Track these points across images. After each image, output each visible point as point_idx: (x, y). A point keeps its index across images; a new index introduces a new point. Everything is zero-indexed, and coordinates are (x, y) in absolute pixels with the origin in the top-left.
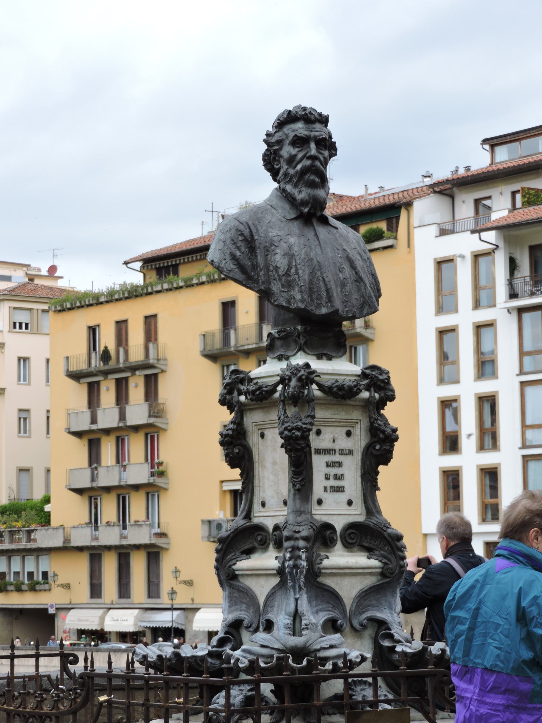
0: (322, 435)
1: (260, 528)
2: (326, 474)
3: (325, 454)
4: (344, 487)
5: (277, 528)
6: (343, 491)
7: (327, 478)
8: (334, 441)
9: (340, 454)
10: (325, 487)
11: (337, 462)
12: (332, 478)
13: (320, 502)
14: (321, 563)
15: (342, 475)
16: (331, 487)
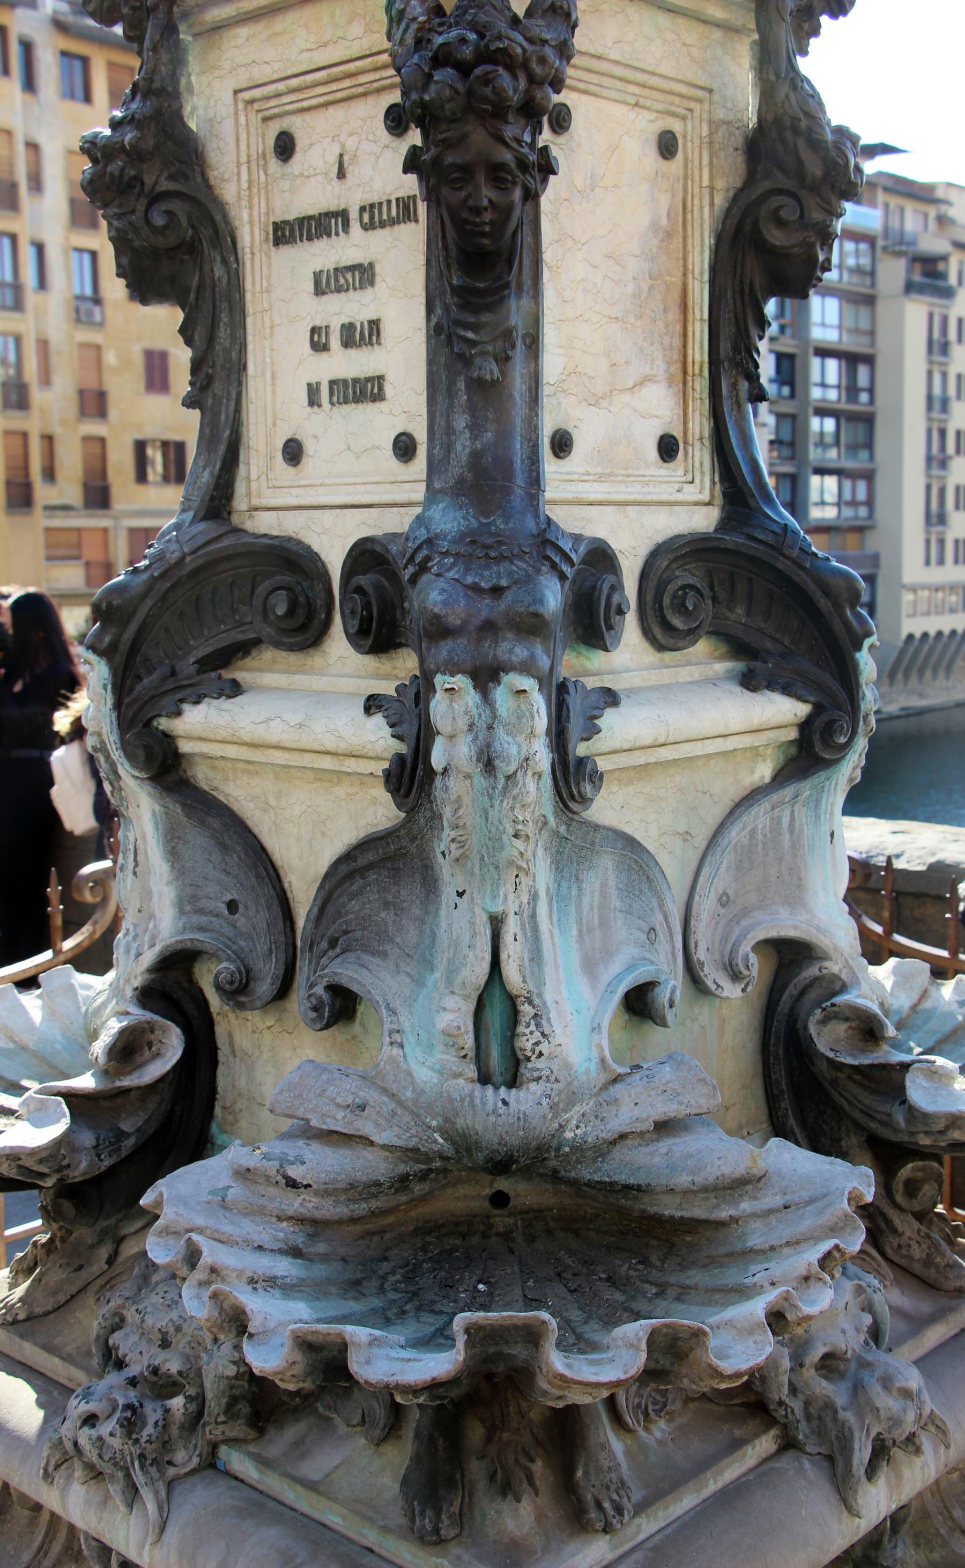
0: (297, 157)
1: (293, 560)
2: (314, 330)
3: (310, 239)
4: (381, 378)
5: (366, 555)
6: (379, 397)
7: (319, 344)
8: (341, 174)
9: (365, 228)
10: (309, 385)
11: (352, 268)
12: (335, 342)
13: (293, 452)
14: (179, 713)
15: (375, 325)
16: (332, 383)
